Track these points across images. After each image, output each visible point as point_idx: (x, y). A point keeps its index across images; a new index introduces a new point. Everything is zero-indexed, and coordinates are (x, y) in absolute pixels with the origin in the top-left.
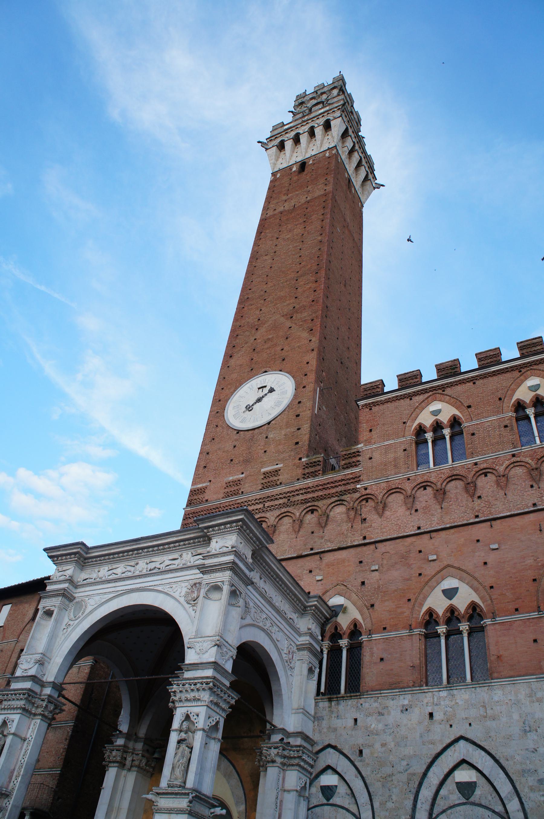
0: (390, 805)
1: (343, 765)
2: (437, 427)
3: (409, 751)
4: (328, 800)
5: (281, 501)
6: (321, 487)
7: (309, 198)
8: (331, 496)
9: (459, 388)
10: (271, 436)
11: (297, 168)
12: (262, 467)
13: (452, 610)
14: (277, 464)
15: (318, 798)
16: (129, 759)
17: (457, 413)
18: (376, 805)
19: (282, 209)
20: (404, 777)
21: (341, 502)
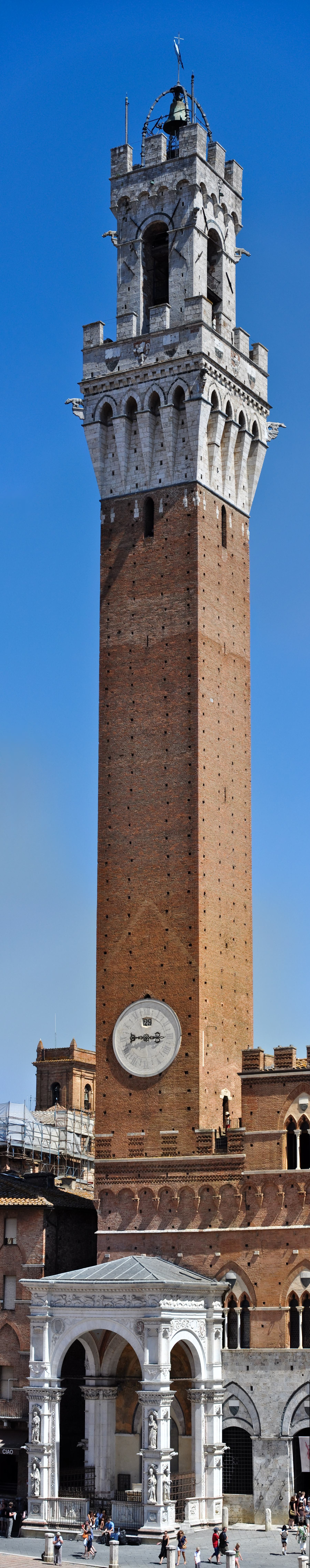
0: (269, 1420)
1: (241, 1395)
3: (280, 1389)
4: (234, 1415)
5: (182, 1174)
6: (212, 1167)
10: (164, 1092)
11: (140, 511)
12: (160, 1129)
14: (173, 1130)
16: (101, 1393)
18: (261, 1420)
19: (128, 637)
20: (276, 1404)
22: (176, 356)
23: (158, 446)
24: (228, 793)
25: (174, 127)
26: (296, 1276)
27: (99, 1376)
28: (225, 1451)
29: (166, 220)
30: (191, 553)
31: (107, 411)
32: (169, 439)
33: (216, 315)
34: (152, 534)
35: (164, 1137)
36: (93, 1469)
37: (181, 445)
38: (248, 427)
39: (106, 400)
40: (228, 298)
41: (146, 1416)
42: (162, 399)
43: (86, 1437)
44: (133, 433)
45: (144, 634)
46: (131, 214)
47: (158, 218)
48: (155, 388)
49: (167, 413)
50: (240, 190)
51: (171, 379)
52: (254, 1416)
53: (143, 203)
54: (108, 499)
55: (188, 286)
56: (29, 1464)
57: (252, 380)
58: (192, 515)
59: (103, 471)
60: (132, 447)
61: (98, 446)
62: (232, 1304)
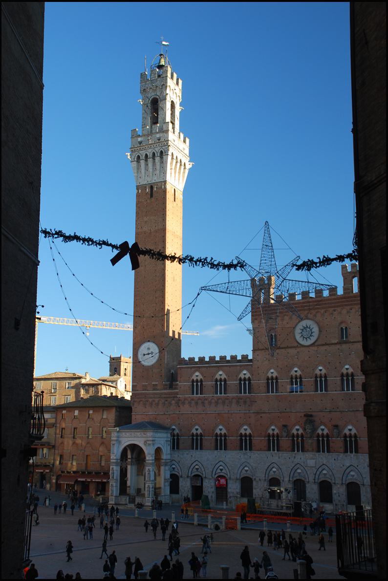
2: (197, 381)
7: (156, 228)
8: (171, 398)
9: (203, 369)
10: (154, 371)
12: (152, 382)
13: (197, 433)
15: (172, 470)
17: (202, 378)
21: (174, 400)
22: (160, 141)
23: (154, 169)
24: (175, 279)
25: (160, 67)
26: (193, 427)
27: (132, 458)
28: (171, 481)
29: (158, 97)
30: (164, 203)
31: (139, 157)
32: (158, 166)
33: (173, 128)
34: (152, 197)
35: (154, 385)
36: (129, 487)
37: (162, 169)
38: (183, 164)
39: (138, 154)
40: (177, 123)
41: (147, 470)
42: (156, 154)
43: (128, 476)
44: (147, 165)
45: (149, 229)
46: (147, 95)
47: (155, 96)
48: (154, 151)
49: (157, 159)
50: (181, 89)
51: (159, 148)
52: (180, 470)
53: (150, 92)
54: (138, 186)
55: (165, 119)
56: (110, 485)
57: (184, 149)
58: (165, 191)
59: (137, 176)
60: (147, 169)
61: (136, 169)
62: (174, 436)
